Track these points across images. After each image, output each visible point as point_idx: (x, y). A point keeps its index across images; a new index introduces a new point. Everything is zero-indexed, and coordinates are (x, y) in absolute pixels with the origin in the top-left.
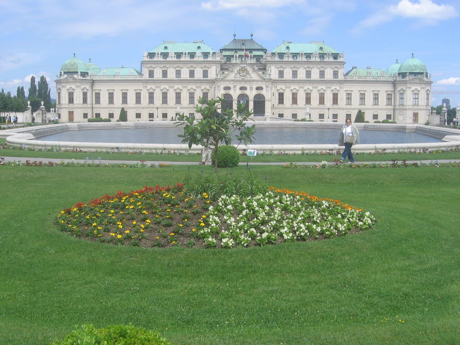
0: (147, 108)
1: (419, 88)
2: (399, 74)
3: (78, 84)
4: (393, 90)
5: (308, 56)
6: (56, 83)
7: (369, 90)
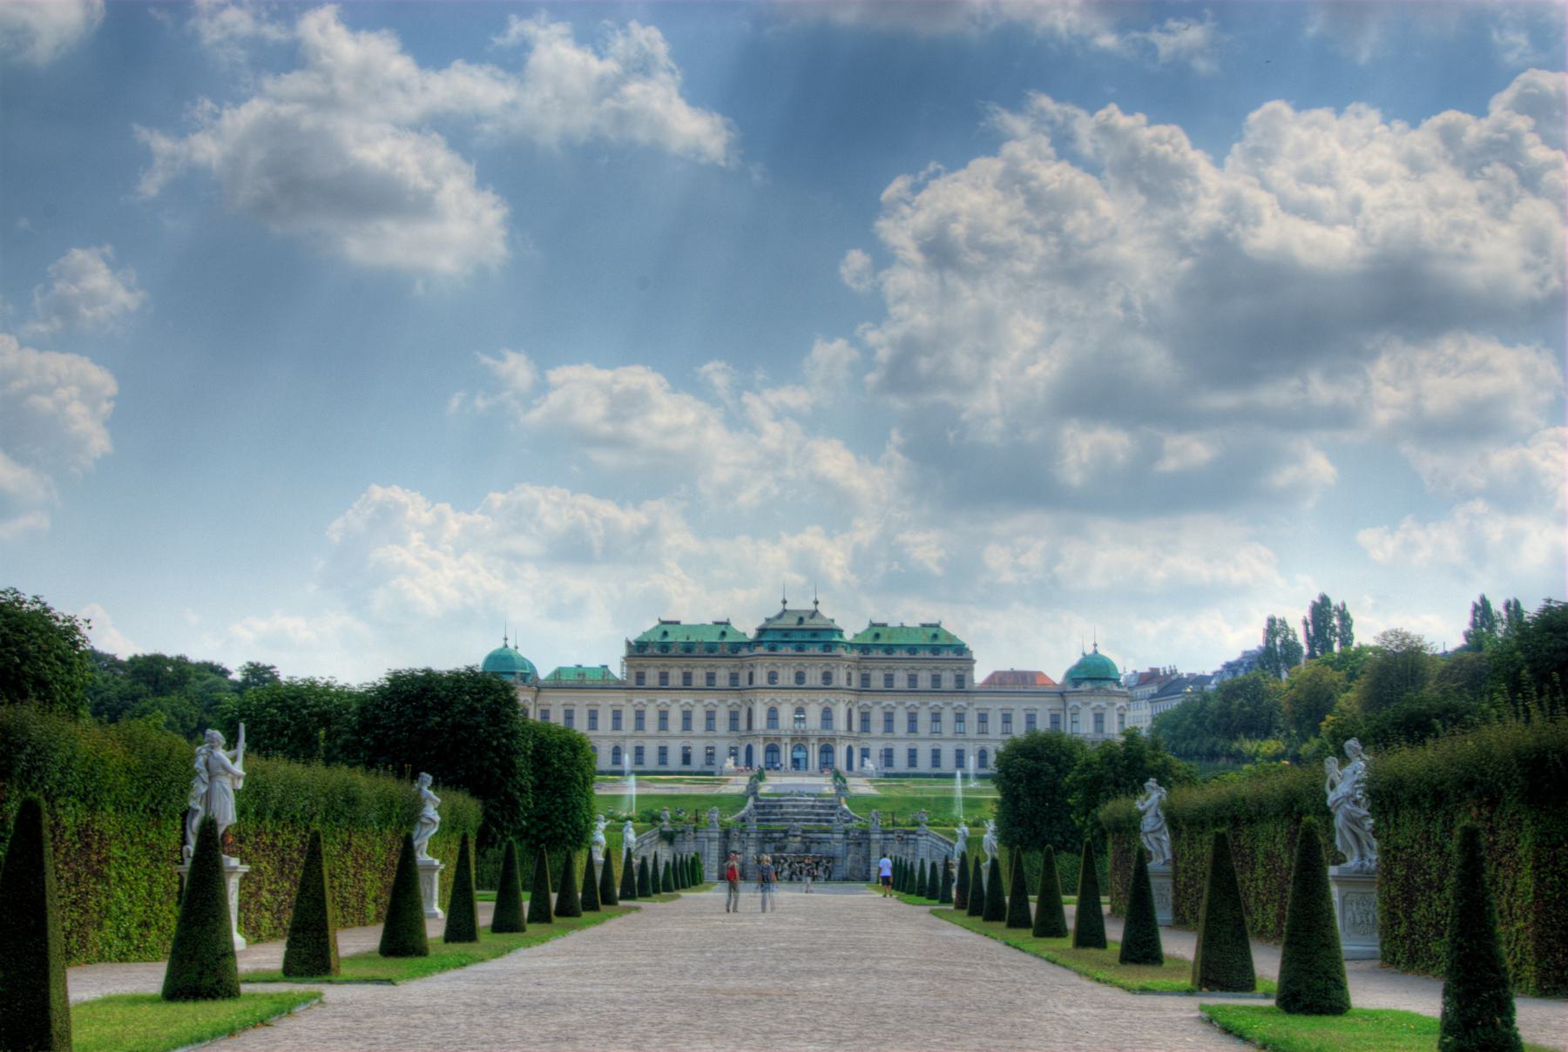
1: (1103, 704)
5: (913, 649)
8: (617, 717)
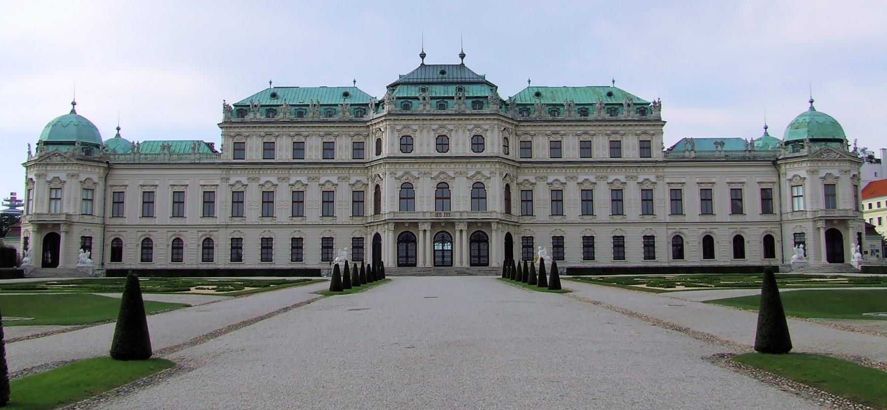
0: (227, 226)
1: (836, 173)
2: (787, 143)
3: (74, 169)
4: (775, 179)
5: (584, 110)
6: (27, 167)
7: (721, 181)
8: (209, 201)
